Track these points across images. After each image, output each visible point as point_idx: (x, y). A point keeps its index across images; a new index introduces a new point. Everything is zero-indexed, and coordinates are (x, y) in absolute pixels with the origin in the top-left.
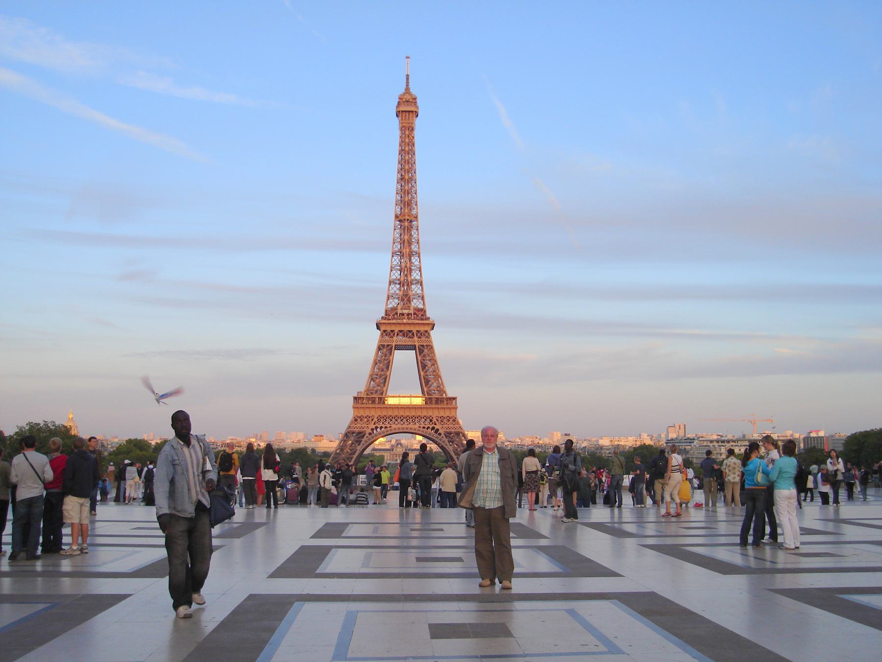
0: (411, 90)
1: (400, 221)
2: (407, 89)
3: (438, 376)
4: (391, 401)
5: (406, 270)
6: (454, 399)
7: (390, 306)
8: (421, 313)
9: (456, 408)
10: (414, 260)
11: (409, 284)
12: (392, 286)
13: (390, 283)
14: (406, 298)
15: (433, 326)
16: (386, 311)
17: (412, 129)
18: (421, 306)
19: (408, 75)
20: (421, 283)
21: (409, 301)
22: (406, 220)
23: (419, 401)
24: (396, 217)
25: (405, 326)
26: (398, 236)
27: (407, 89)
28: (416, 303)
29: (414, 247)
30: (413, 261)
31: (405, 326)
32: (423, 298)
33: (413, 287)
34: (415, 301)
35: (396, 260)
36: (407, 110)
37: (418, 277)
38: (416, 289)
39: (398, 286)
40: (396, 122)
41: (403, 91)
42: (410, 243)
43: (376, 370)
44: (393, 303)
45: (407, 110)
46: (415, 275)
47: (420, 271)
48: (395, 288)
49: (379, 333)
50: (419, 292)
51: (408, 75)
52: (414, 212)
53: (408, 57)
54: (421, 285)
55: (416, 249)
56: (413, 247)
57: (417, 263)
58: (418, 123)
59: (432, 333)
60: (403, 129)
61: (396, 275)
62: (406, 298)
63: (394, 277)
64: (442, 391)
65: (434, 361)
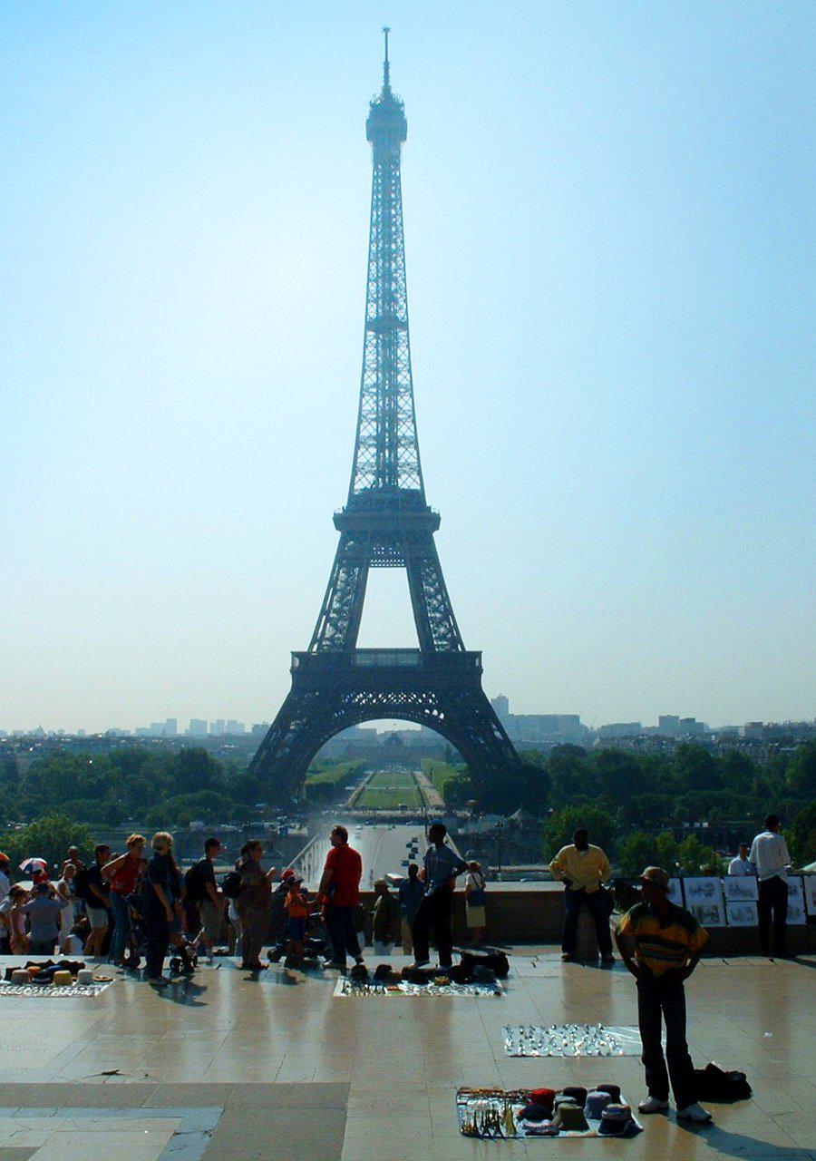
0: (393, 91)
1: (377, 331)
3: (448, 612)
4: (361, 661)
5: (388, 418)
6: (478, 655)
7: (359, 486)
8: (417, 498)
9: (479, 671)
10: (403, 402)
11: (394, 446)
12: (362, 449)
14: (388, 470)
15: (435, 521)
16: (352, 497)
18: (416, 486)
19: (387, 64)
21: (397, 476)
22: (387, 326)
23: (412, 661)
24: (369, 325)
25: (388, 524)
26: (371, 357)
28: (407, 482)
29: (402, 379)
30: (401, 403)
31: (388, 524)
32: (420, 474)
33: (401, 450)
34: (404, 477)
35: (370, 403)
36: (387, 124)
37: (410, 434)
38: (405, 455)
39: (373, 450)
40: (367, 150)
41: (379, 92)
42: (397, 372)
43: (336, 605)
44: (365, 482)
45: (387, 124)
46: (404, 430)
47: (414, 422)
48: (368, 455)
49: (339, 533)
50: (413, 460)
51: (387, 64)
52: (400, 315)
53: (386, 30)
54: (417, 447)
55: (405, 382)
56: (400, 378)
57: (407, 407)
58: (405, 148)
59: (436, 535)
61: (370, 429)
62: (388, 470)
63: (364, 434)
64: (457, 640)
65: (442, 588)
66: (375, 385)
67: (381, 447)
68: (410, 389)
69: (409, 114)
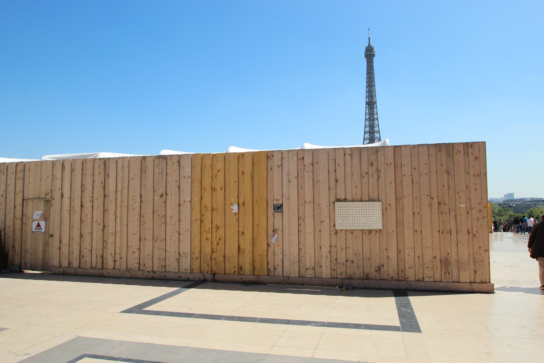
2: (369, 44)
10: (376, 122)
11: (373, 133)
13: (365, 133)
17: (372, 62)
19: (369, 38)
20: (379, 132)
22: (371, 104)
24: (367, 103)
27: (369, 44)
35: (367, 123)
36: (370, 54)
40: (365, 59)
42: (374, 115)
45: (370, 54)
46: (376, 129)
48: (367, 136)
51: (369, 38)
52: (375, 100)
58: (375, 59)
60: (368, 62)
66: (369, 118)
67: (370, 133)
68: (377, 119)
69: (375, 49)
